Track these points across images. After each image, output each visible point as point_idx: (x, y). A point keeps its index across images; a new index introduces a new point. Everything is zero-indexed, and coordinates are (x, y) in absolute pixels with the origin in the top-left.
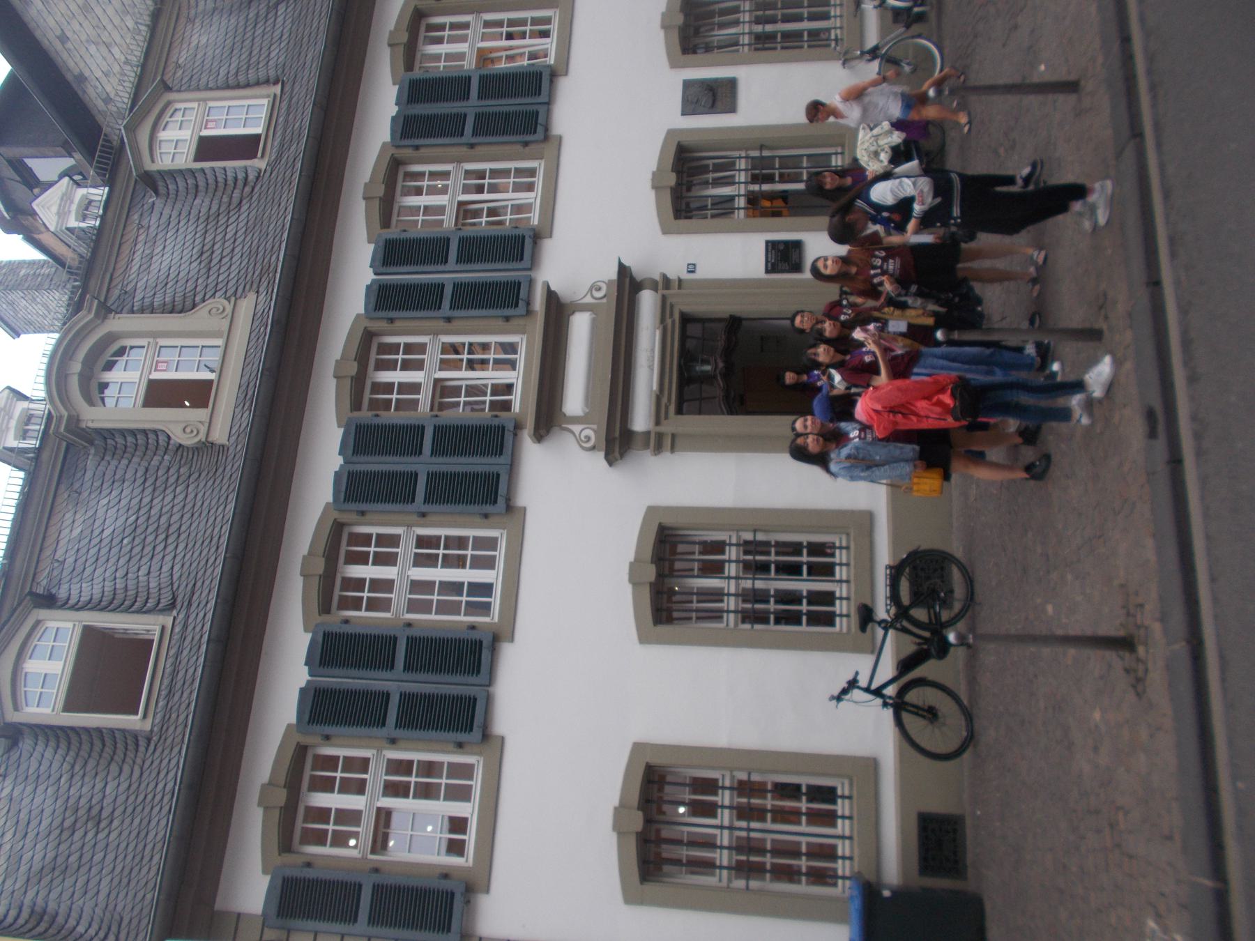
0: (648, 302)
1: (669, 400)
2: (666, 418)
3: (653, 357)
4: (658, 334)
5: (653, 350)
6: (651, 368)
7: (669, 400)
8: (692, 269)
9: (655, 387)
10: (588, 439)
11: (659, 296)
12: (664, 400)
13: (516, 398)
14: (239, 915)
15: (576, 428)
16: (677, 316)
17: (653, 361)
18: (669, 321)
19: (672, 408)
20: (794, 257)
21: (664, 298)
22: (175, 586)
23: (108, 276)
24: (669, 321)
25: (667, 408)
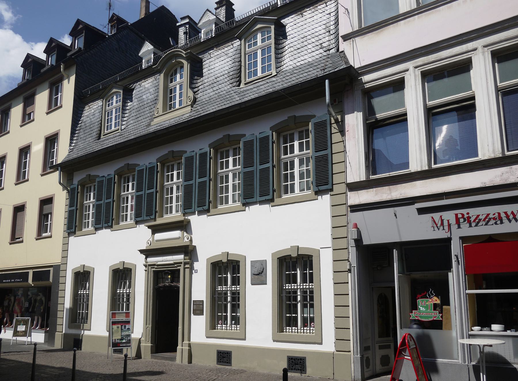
0: (180, 257)
1: (156, 268)
2: (152, 268)
3: (166, 261)
4: (172, 262)
5: (167, 261)
6: (162, 261)
7: (156, 268)
8: (196, 272)
9: (159, 263)
10: (148, 244)
11: (182, 261)
12: (156, 267)
13: (169, 215)
14: (73, 179)
15: (151, 240)
16: (178, 268)
17: (165, 261)
18: (176, 265)
19: (154, 269)
20: (198, 312)
21: (181, 263)
22: (127, 128)
23: (217, 44)
24: (176, 265)
25: (154, 268)
